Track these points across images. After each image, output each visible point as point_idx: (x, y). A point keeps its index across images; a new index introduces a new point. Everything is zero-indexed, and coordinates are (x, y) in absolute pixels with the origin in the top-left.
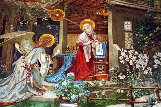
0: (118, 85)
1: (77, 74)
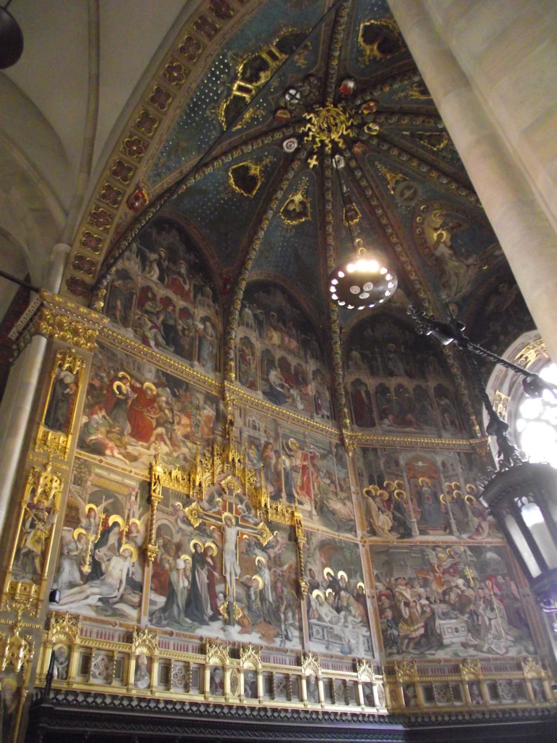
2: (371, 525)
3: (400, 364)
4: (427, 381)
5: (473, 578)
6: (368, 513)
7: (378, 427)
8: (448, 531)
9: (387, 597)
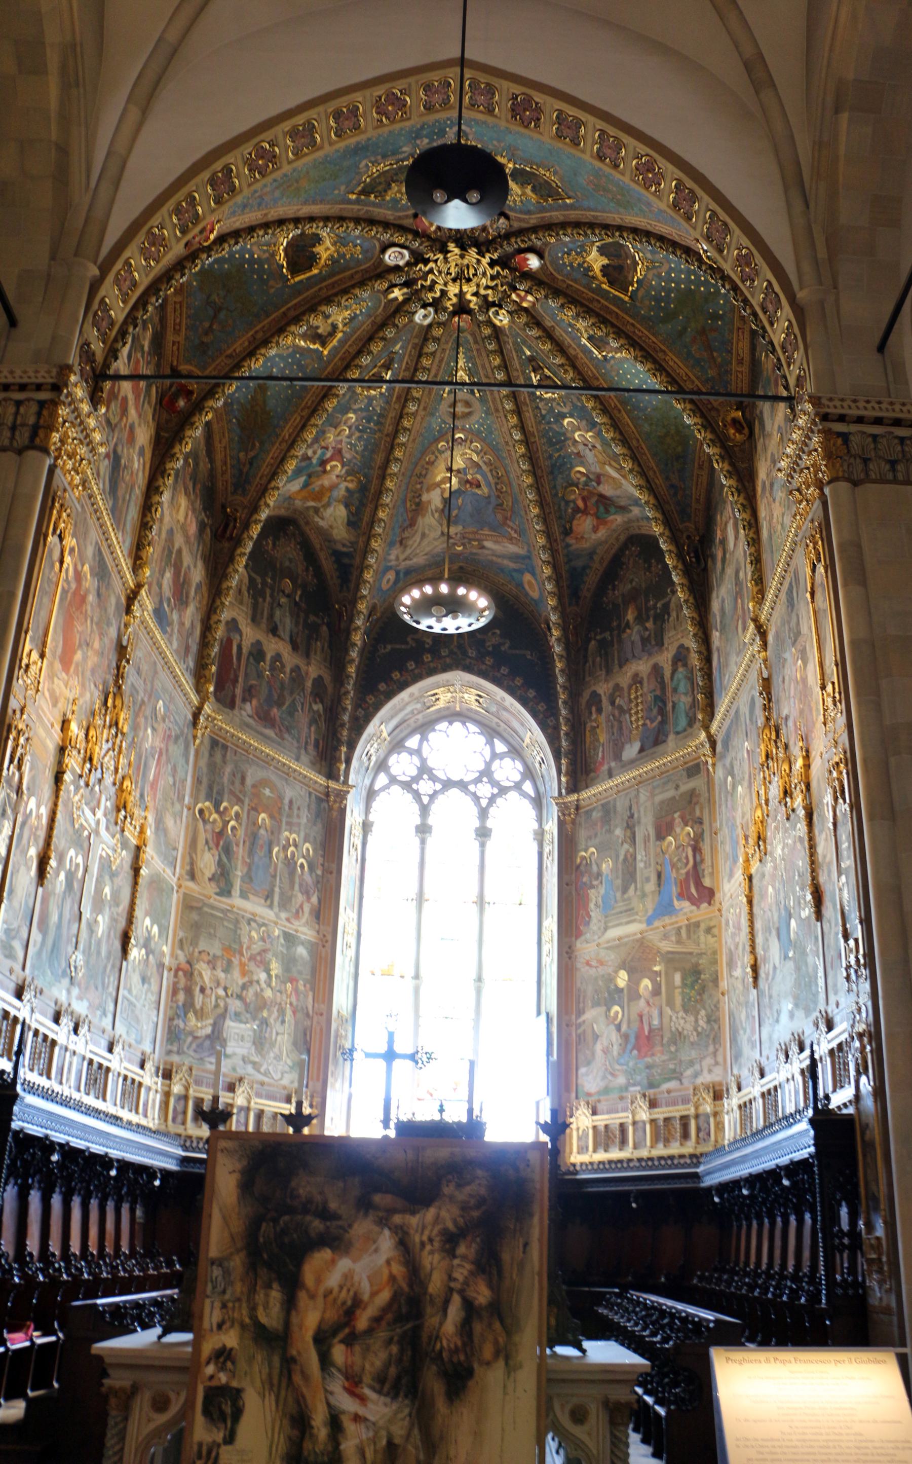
0: (670, 1060)
1: (639, 1051)
2: (192, 864)
3: (288, 621)
4: (308, 664)
5: (276, 976)
6: (192, 844)
7: (236, 711)
8: (269, 902)
9: (185, 973)
